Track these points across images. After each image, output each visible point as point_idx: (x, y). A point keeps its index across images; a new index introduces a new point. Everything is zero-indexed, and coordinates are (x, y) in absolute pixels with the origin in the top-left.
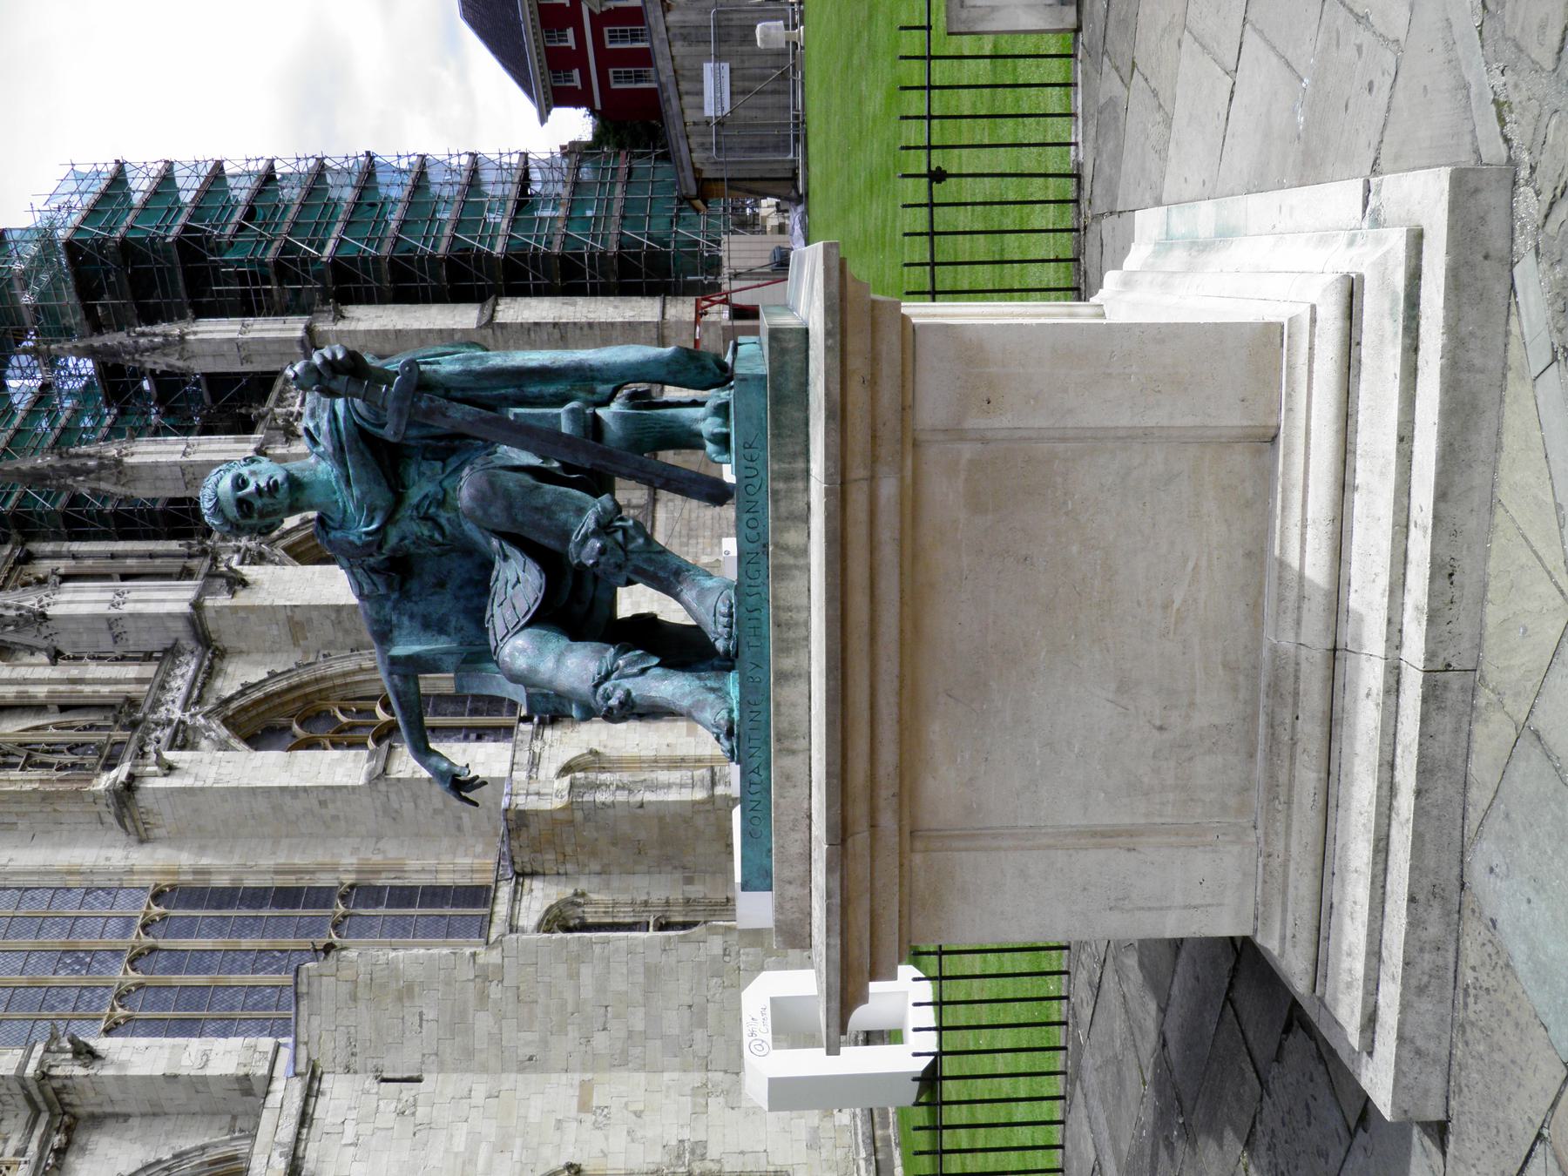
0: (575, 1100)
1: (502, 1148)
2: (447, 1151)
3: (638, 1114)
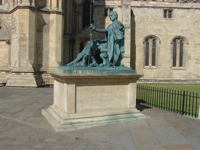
0: (197, 43)
1: (191, 34)
2: (191, 28)
3: (195, 51)
